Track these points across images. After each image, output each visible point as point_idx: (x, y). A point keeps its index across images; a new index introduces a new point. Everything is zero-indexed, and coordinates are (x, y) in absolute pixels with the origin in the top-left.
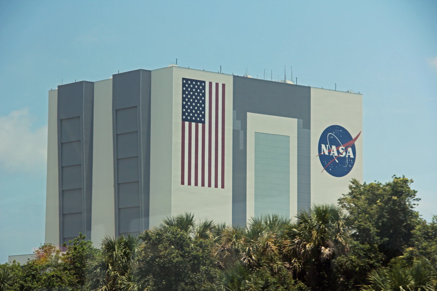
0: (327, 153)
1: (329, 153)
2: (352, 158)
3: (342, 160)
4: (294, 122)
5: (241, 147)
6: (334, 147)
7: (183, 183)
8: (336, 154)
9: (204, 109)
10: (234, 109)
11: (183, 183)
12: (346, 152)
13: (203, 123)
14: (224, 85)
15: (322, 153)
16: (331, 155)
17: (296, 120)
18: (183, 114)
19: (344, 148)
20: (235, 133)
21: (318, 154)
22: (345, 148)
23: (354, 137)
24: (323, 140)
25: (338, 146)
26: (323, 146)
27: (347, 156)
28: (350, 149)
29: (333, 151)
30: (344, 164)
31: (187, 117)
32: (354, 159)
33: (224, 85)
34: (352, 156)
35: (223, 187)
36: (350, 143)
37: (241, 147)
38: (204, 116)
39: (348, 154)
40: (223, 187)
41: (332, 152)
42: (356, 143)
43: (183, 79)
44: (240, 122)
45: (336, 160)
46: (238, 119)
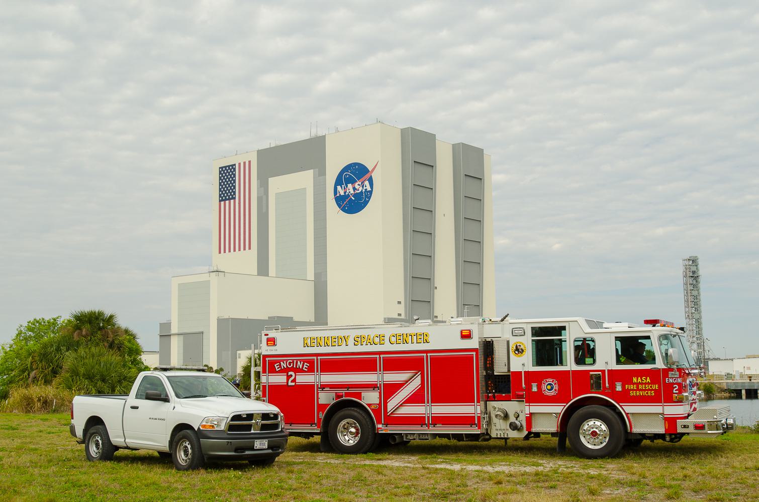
0: (342, 193)
1: (345, 193)
2: (369, 191)
3: (358, 196)
4: (310, 174)
5: (264, 211)
6: (350, 186)
7: (220, 253)
8: (352, 192)
9: (235, 187)
10: (258, 180)
11: (220, 253)
12: (363, 187)
13: (235, 198)
14: (250, 162)
15: (338, 195)
16: (347, 193)
17: (312, 170)
18: (220, 196)
19: (360, 183)
20: (260, 199)
21: (334, 197)
22: (362, 183)
23: (370, 170)
25: (353, 182)
27: (364, 191)
28: (367, 183)
29: (349, 190)
30: (361, 199)
31: (222, 198)
32: (371, 192)
33: (250, 162)
34: (369, 189)
35: (250, 248)
36: (368, 176)
37: (264, 211)
38: (235, 194)
39: (365, 188)
40: (250, 248)
41: (348, 191)
42: (374, 175)
43: (220, 168)
44: (263, 188)
45: (352, 197)
46: (261, 187)
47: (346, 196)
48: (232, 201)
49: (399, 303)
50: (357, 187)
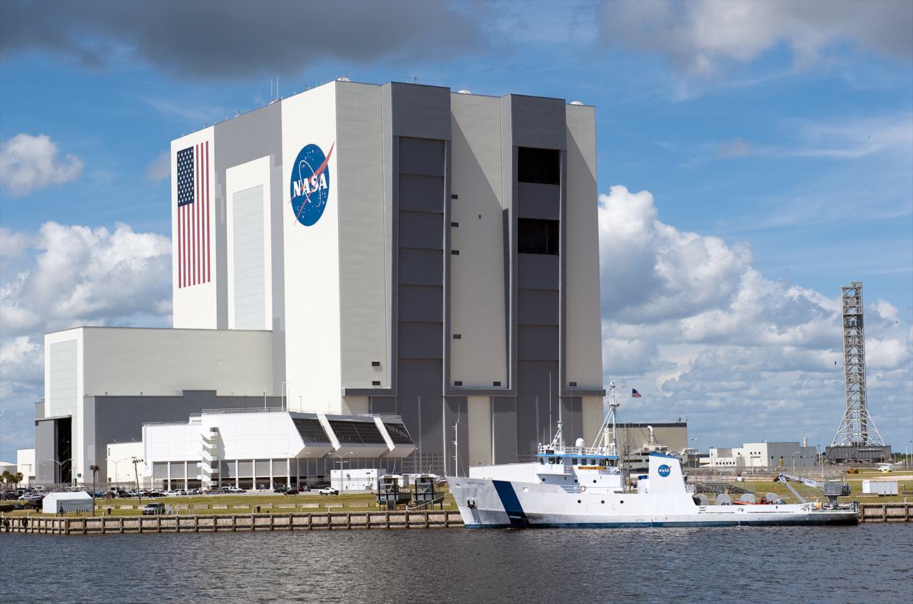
0: (299, 194)
3: (314, 196)
5: (222, 221)
6: (306, 180)
7: (180, 287)
8: (309, 192)
11: (180, 287)
13: (192, 201)
14: (207, 142)
17: (269, 156)
19: (316, 177)
20: (217, 201)
24: (295, 178)
25: (309, 176)
26: (295, 183)
27: (320, 189)
28: (323, 177)
33: (207, 142)
34: (325, 187)
35: (209, 281)
36: (322, 167)
39: (321, 185)
40: (209, 281)
43: (178, 153)
44: (220, 185)
47: (303, 198)
48: (191, 205)
49: (376, 364)
50: (313, 183)
